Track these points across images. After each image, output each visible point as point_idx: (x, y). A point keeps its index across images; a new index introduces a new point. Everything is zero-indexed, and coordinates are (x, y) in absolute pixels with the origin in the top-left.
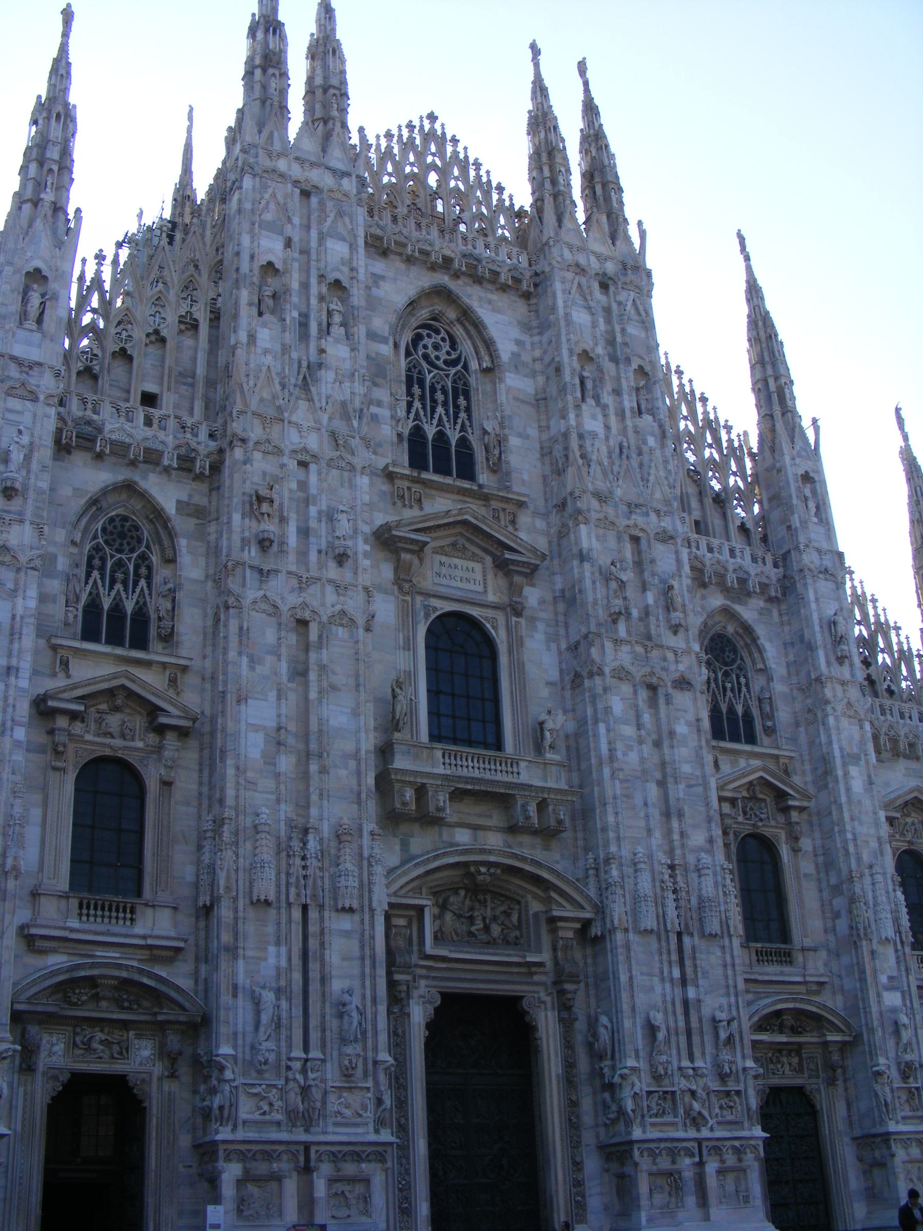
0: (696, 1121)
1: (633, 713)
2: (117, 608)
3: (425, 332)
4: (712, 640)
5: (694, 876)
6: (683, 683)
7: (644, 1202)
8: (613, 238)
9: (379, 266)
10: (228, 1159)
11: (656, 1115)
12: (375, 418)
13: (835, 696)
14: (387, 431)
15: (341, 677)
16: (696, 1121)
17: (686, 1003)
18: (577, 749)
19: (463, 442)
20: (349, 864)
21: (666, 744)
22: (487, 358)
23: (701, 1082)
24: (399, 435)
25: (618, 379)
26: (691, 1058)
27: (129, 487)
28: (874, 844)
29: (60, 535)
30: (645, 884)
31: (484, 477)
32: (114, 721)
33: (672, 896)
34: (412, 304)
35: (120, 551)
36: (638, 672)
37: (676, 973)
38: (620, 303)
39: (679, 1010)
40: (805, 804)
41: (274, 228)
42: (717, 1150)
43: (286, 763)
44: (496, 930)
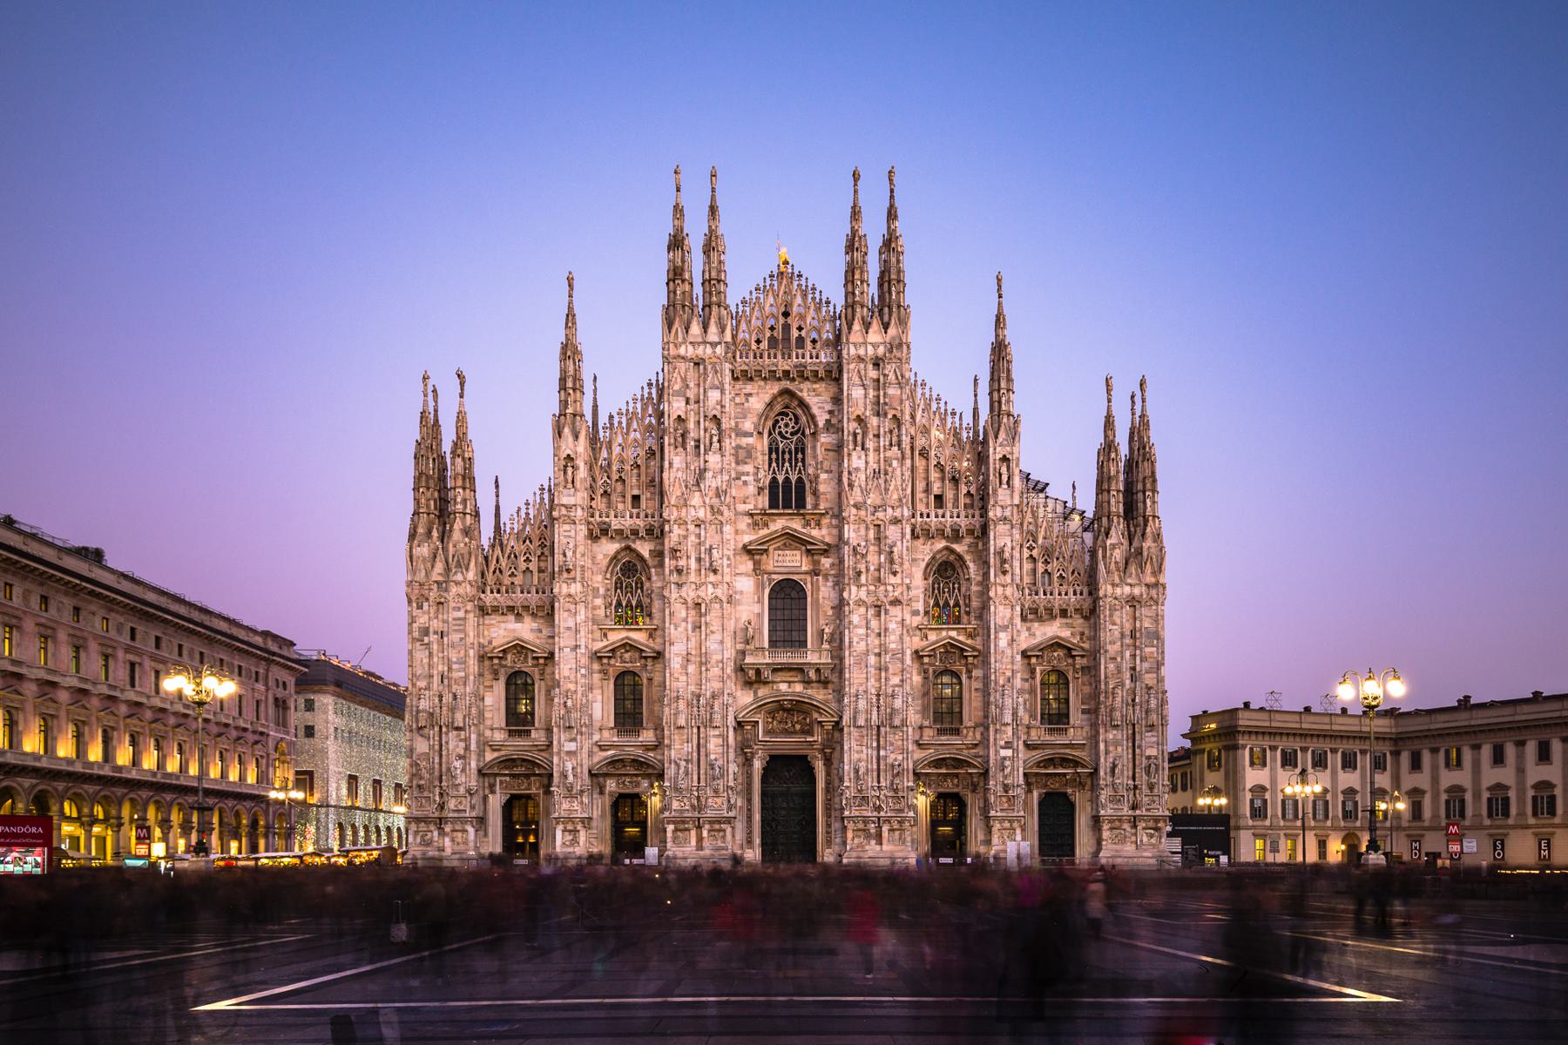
0: (879, 809)
6: (896, 602)
9: (749, 388)
12: (745, 483)
14: (752, 489)
15: (715, 626)
16: (879, 809)
18: (842, 640)
19: (800, 480)
20: (716, 708)
24: (761, 489)
28: (1009, 674)
29: (600, 578)
30: (862, 704)
32: (627, 656)
34: (770, 405)
43: (691, 668)
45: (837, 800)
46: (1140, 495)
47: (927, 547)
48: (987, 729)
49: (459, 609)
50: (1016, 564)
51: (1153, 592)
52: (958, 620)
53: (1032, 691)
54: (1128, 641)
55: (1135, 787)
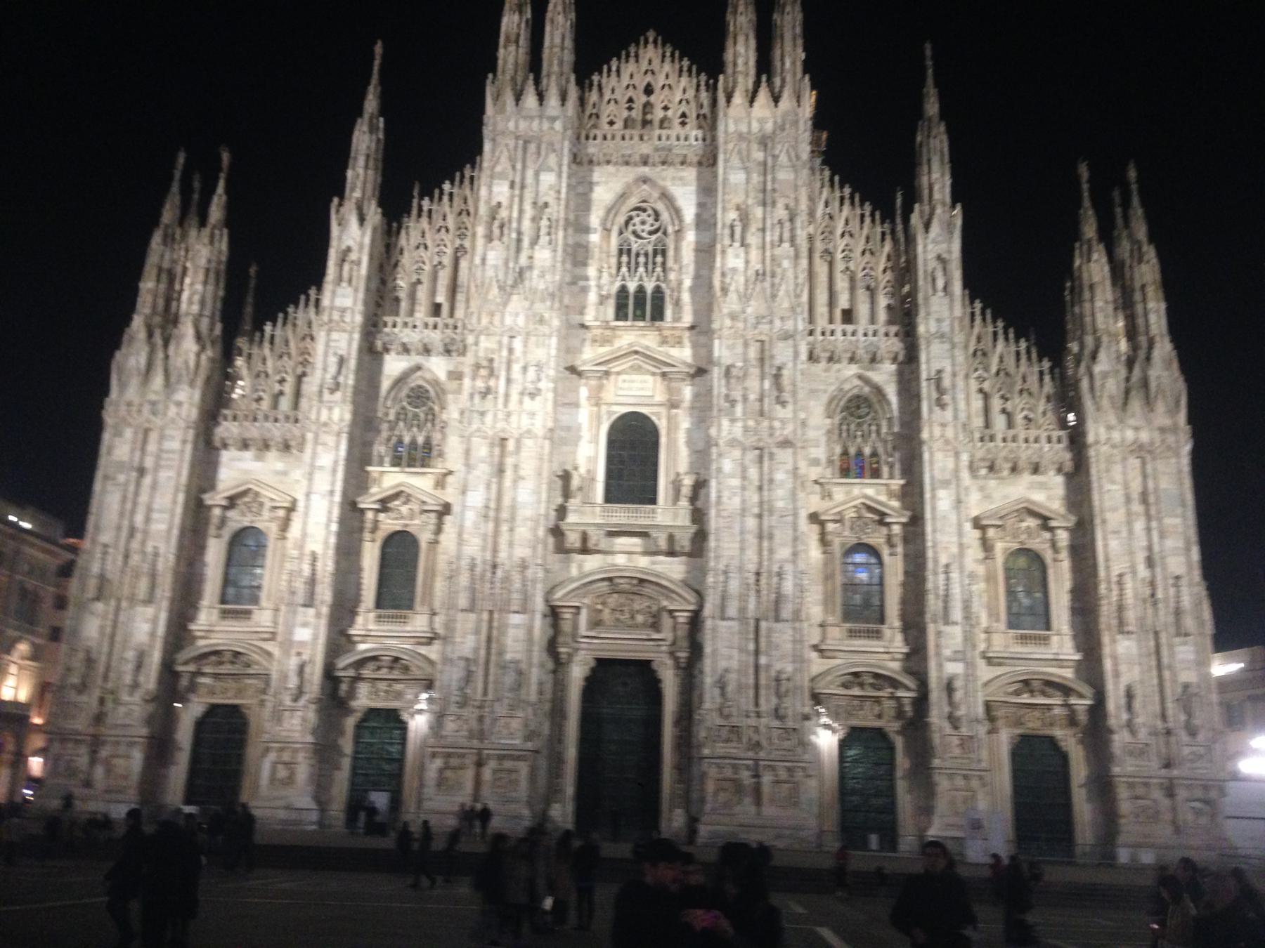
1: (739, 469)
2: (413, 443)
3: (634, 213)
4: (850, 401)
5: (775, 580)
6: (786, 443)
7: (709, 798)
8: (776, 99)
10: (434, 755)
11: (727, 741)
13: (931, 437)
14: (592, 297)
17: (757, 667)
19: (658, 291)
21: (766, 487)
22: (676, 222)
23: (763, 720)
25: (764, 219)
26: (757, 704)
27: (419, 368)
28: (955, 549)
30: (734, 586)
31: (669, 312)
33: (752, 594)
34: (623, 196)
35: (416, 407)
36: (751, 440)
37: (751, 646)
38: (775, 157)
39: (751, 671)
40: (904, 520)
41: (502, 176)
42: (773, 768)
44: (640, 618)
45: (695, 729)
46: (1139, 308)
47: (833, 374)
48: (922, 631)
49: (172, 438)
50: (961, 396)
51: (1171, 439)
52: (876, 474)
53: (990, 578)
54: (1137, 507)
55: (1168, 732)
